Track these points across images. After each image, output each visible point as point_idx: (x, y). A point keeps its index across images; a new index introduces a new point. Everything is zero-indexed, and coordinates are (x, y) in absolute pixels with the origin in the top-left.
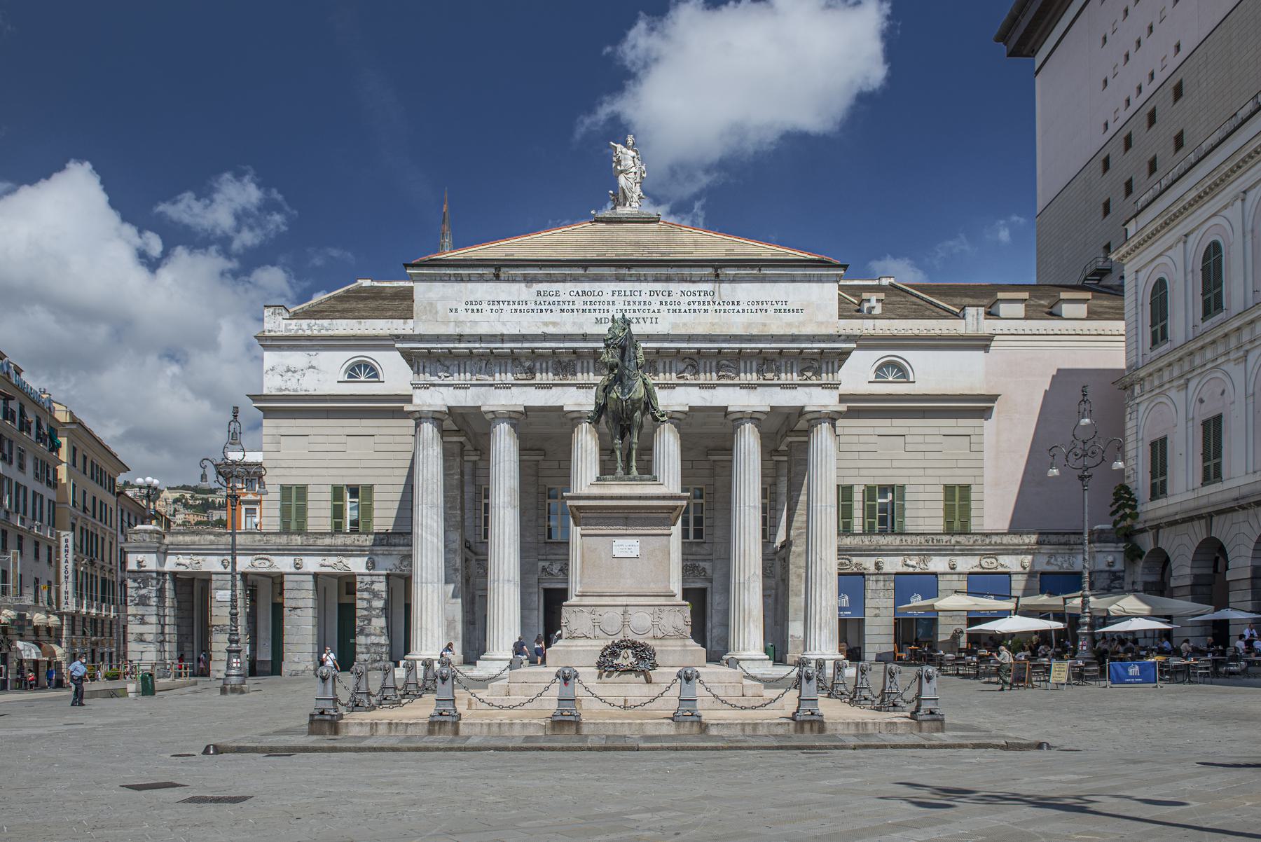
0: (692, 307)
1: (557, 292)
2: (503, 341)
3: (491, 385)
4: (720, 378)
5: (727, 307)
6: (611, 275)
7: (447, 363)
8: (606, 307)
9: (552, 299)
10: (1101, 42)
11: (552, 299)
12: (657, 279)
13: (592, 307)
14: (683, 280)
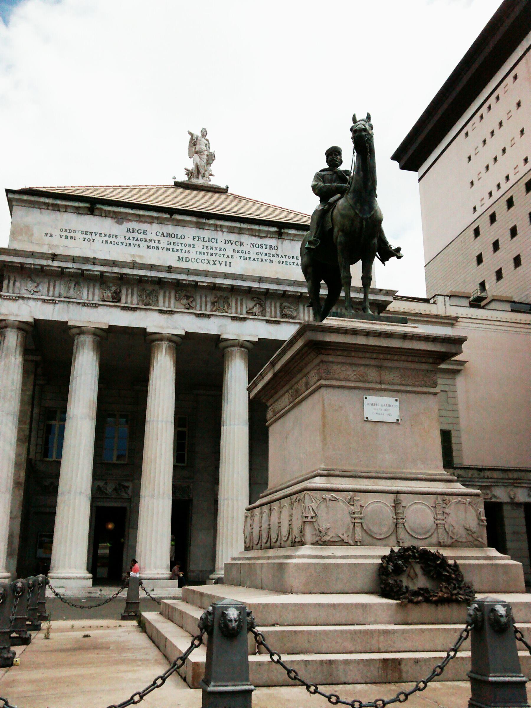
0: (260, 257)
2: (94, 264)
3: (79, 303)
4: (284, 316)
5: (288, 260)
6: (191, 222)
7: (38, 280)
8: (187, 248)
9: (140, 236)
10: (467, 159)
11: (140, 236)
12: (231, 230)
13: (175, 247)
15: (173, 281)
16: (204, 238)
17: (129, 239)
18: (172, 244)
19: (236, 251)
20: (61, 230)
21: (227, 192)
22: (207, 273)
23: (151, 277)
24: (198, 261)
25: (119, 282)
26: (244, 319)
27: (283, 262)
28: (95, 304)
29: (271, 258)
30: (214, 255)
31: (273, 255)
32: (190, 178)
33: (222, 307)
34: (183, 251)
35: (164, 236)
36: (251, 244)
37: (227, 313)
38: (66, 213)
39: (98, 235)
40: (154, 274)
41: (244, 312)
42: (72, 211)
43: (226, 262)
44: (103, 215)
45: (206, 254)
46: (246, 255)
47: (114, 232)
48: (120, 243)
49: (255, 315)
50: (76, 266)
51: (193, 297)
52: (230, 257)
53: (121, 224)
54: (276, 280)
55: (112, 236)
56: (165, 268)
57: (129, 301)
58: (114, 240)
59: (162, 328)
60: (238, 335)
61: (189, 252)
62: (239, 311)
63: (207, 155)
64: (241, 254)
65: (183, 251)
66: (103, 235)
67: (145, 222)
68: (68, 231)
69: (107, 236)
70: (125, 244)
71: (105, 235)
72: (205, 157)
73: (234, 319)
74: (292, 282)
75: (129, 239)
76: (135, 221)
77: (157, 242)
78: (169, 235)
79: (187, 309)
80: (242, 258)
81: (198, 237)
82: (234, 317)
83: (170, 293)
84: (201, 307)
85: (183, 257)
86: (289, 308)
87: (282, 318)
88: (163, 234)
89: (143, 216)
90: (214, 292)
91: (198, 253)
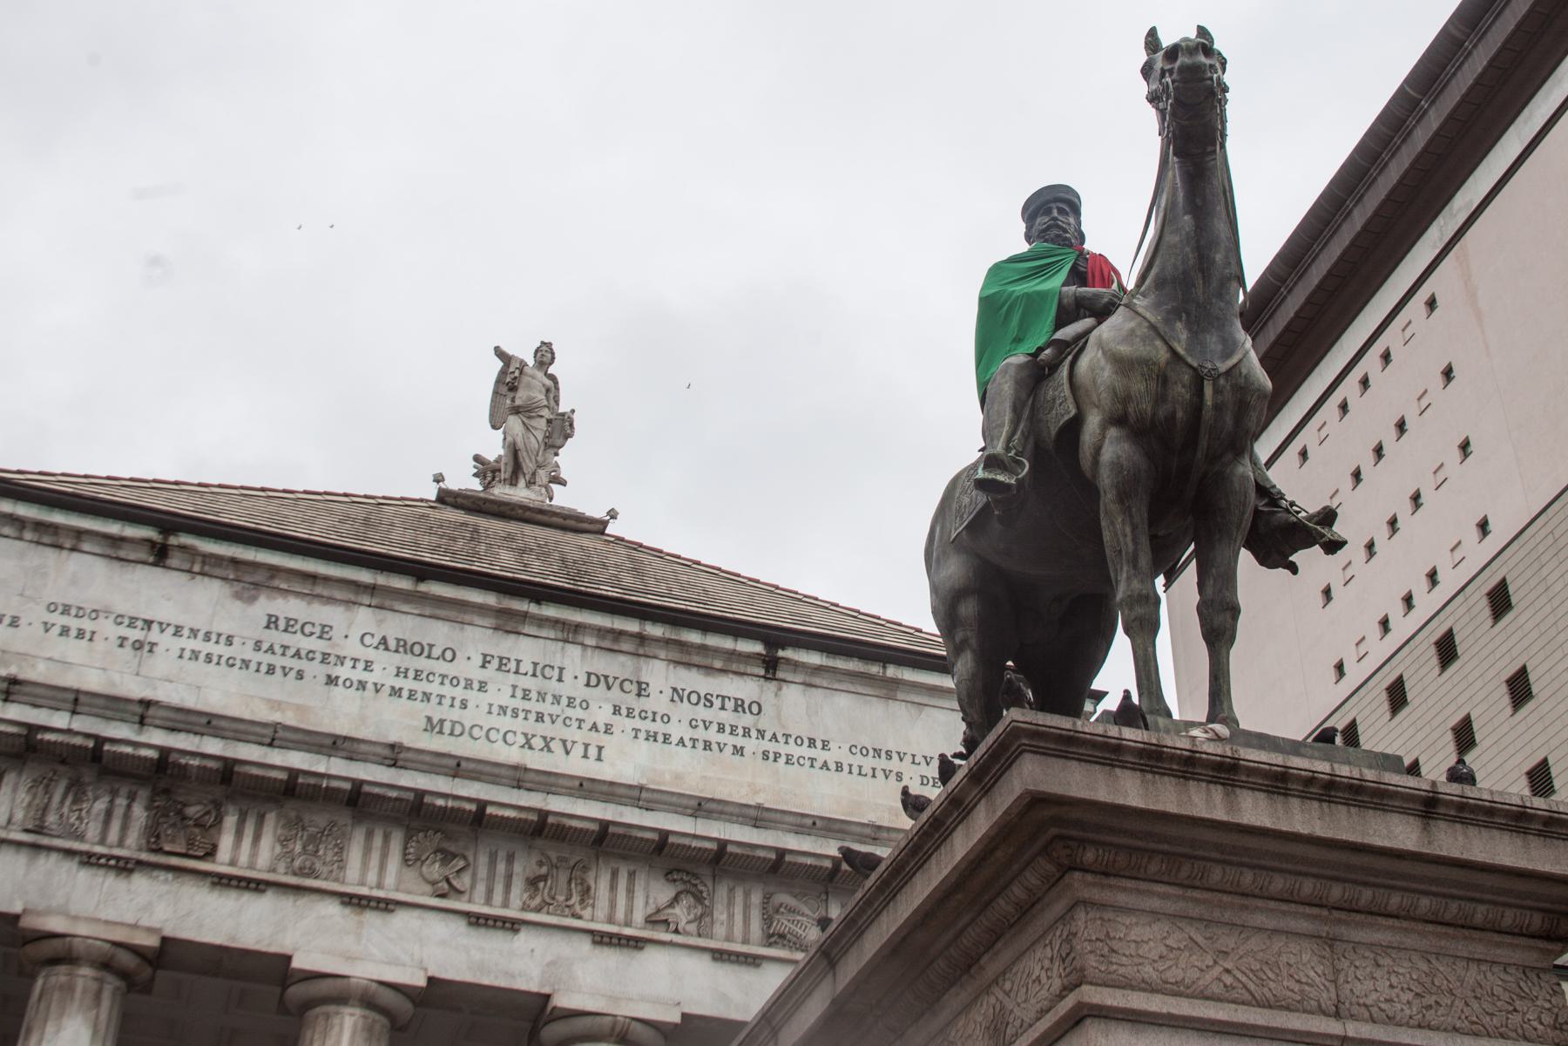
0: (700, 733)
1: (325, 632)
3: (69, 853)
5: (792, 749)
6: (482, 609)
8: (459, 692)
9: (306, 644)
12: (611, 641)
13: (421, 687)
14: (685, 657)
15: (405, 795)
16: (518, 662)
17: (271, 649)
18: (411, 674)
19: (624, 711)
20: (51, 608)
21: (603, 533)
22: (519, 777)
23: (330, 777)
24: (493, 735)
25: (219, 791)
26: (636, 944)
27: (777, 756)
28: (127, 860)
29: (740, 741)
30: (546, 718)
31: (747, 733)
32: (487, 487)
33: (561, 898)
34: (447, 702)
35: (387, 649)
36: (675, 690)
37: (580, 917)
38: (75, 555)
39: (171, 630)
40: (337, 767)
41: (639, 917)
42: (98, 550)
43: (586, 746)
44: (197, 568)
45: (522, 715)
46: (653, 727)
47: (225, 628)
48: (238, 663)
49: (676, 931)
50: (82, 724)
51: (465, 858)
52: (602, 728)
53: (252, 600)
54: (753, 813)
55: (214, 637)
56: (379, 750)
57: (244, 858)
58: (220, 649)
59: (350, 958)
60: (615, 999)
61: (464, 705)
62: (620, 914)
63: (549, 421)
64: (638, 723)
65: (447, 702)
66: (186, 632)
67: (330, 600)
68: (73, 612)
69: (201, 635)
70: (253, 666)
71: (194, 633)
72: (542, 424)
73: (602, 939)
74: (809, 822)
75: (271, 649)
76: (298, 594)
77: (361, 665)
78: (404, 646)
79: (442, 896)
80: (642, 735)
81: (501, 659)
82: (602, 934)
83: (387, 838)
84: (490, 892)
85: (442, 722)
86: (792, 911)
87: (770, 945)
88: (384, 641)
89: (327, 579)
90: (539, 842)
91: (495, 710)
